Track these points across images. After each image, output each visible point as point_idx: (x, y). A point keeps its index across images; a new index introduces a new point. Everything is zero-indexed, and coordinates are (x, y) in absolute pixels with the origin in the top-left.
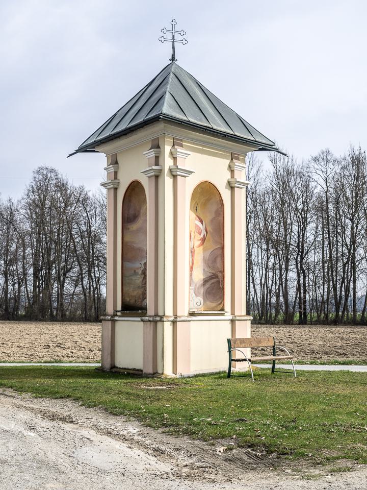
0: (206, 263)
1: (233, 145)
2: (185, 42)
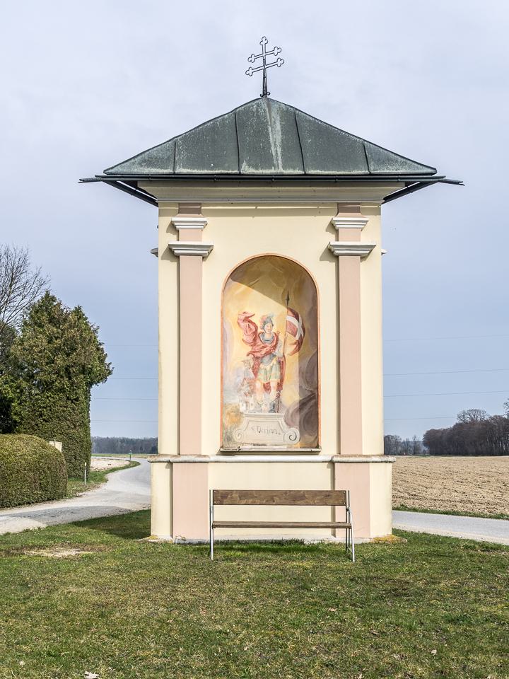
0: (303, 377)
1: (331, 191)
2: (279, 63)
